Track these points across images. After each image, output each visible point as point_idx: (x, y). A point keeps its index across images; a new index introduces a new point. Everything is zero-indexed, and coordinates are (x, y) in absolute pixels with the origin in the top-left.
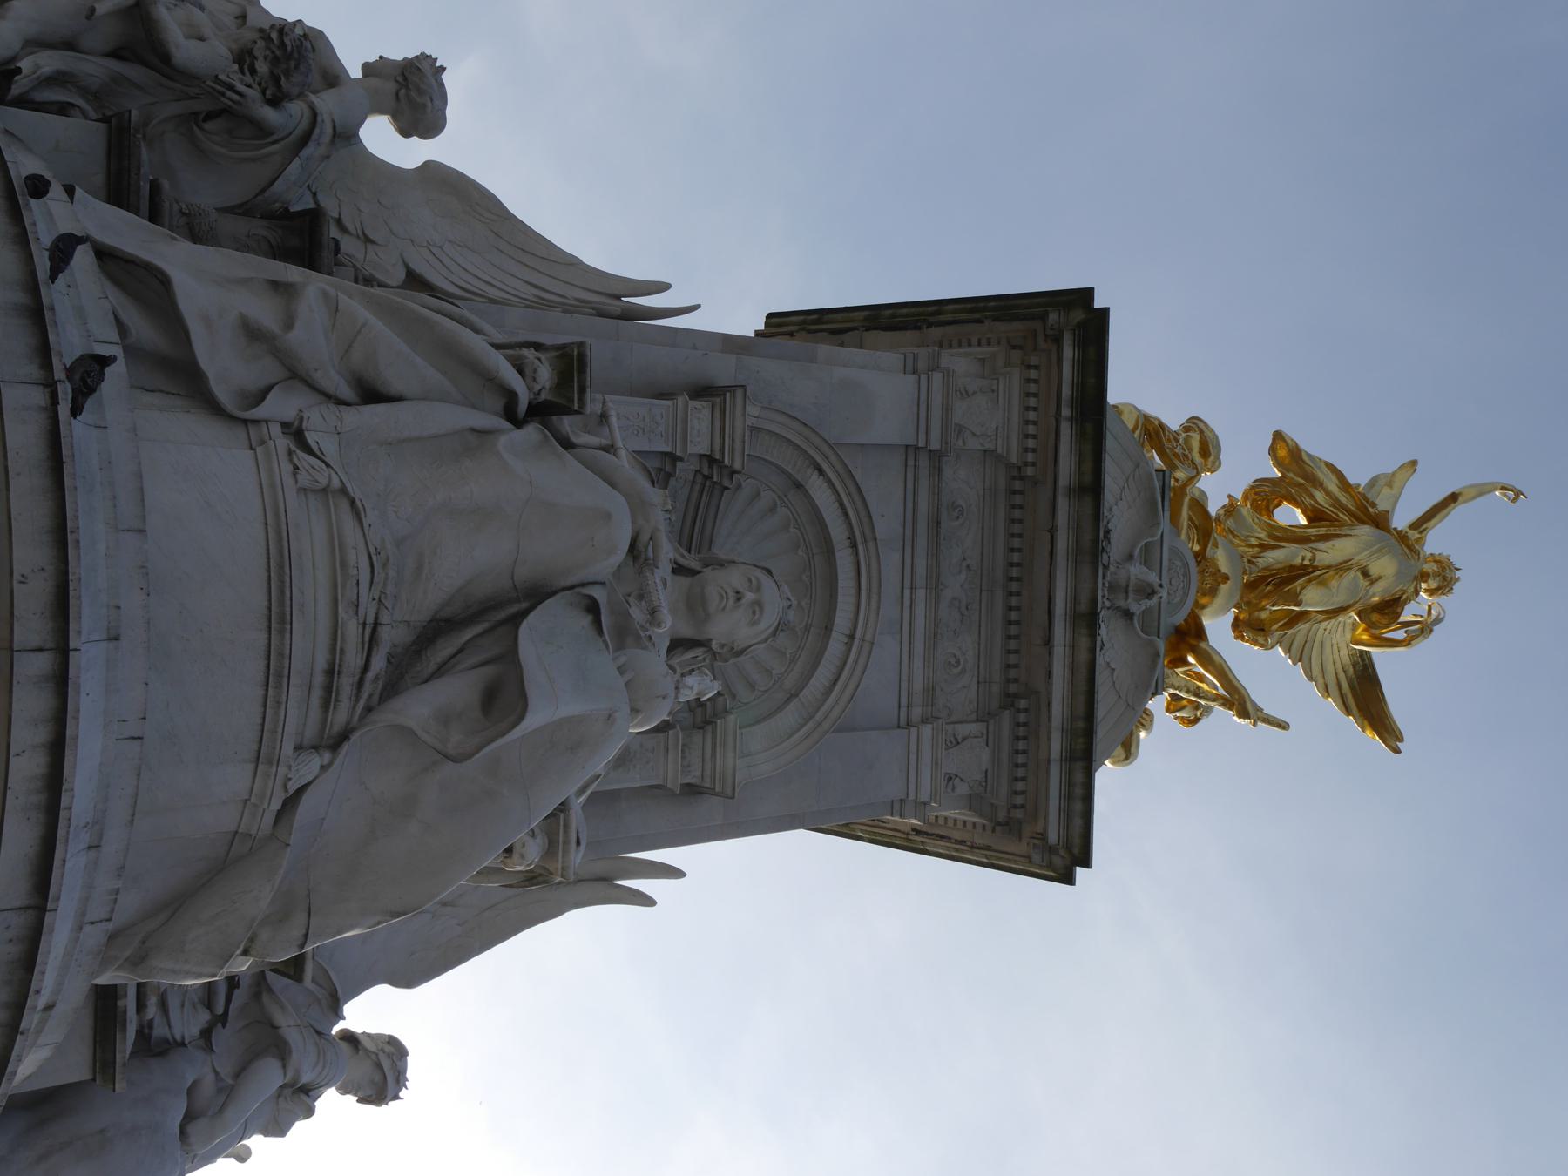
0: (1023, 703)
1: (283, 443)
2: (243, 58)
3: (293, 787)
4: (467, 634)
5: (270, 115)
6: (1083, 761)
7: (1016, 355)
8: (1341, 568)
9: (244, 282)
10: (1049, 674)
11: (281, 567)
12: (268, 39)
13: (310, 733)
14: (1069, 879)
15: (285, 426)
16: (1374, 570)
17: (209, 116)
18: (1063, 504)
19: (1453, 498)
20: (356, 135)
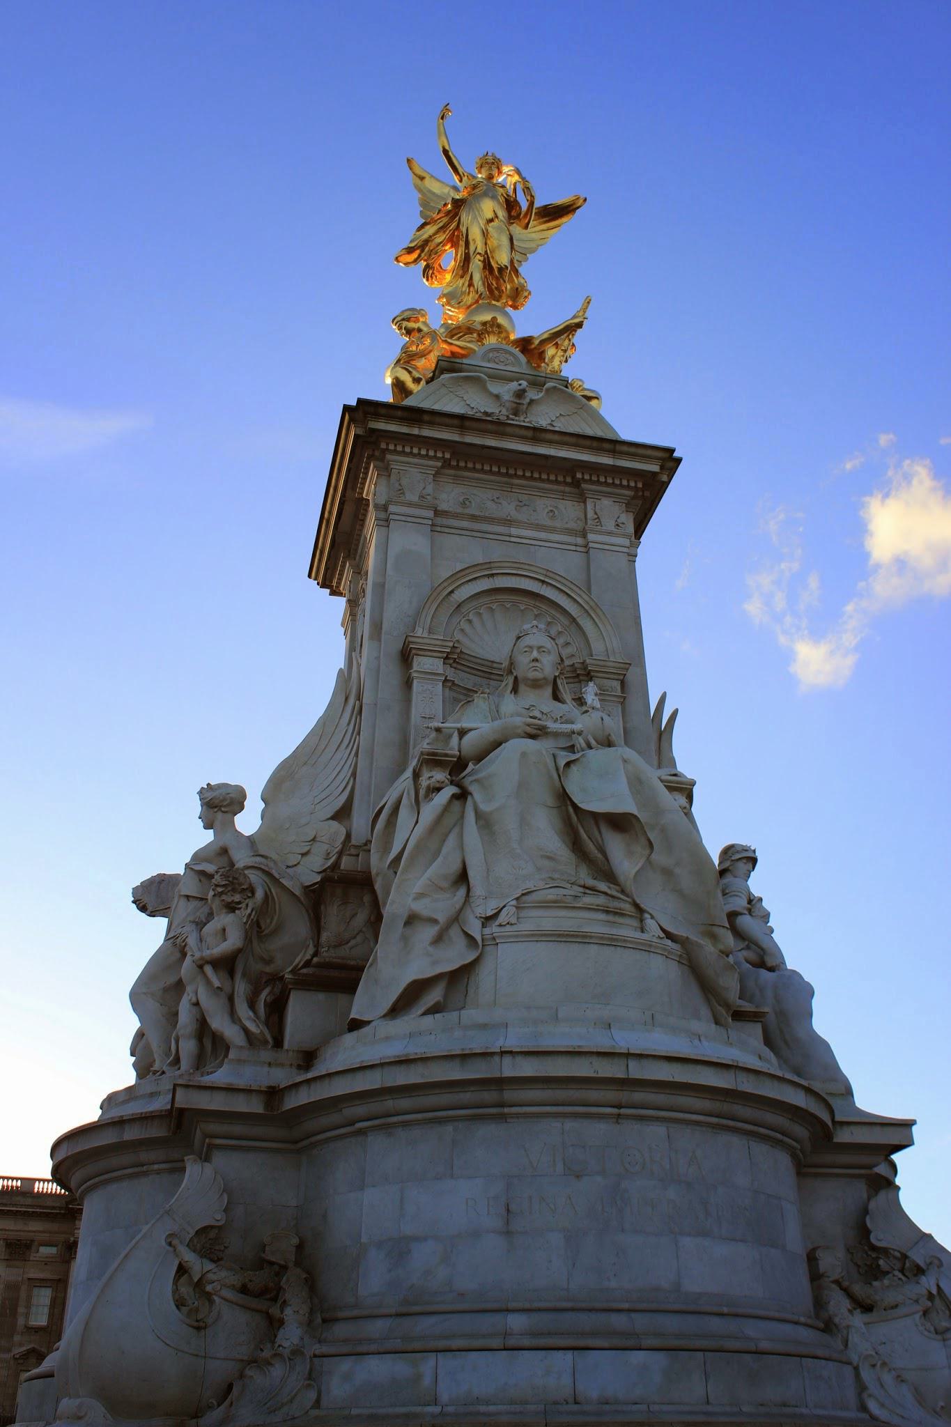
0: (579, 476)
1: (493, 929)
2: (231, 908)
3: (662, 935)
4: (584, 836)
5: (259, 894)
6: (614, 445)
8: (485, 234)
9: (405, 939)
10: (565, 459)
11: (559, 935)
12: (222, 893)
13: (635, 923)
14: (679, 461)
15: (484, 926)
16: (490, 215)
17: (259, 926)
18: (469, 439)
19: (446, 152)
20: (248, 837)
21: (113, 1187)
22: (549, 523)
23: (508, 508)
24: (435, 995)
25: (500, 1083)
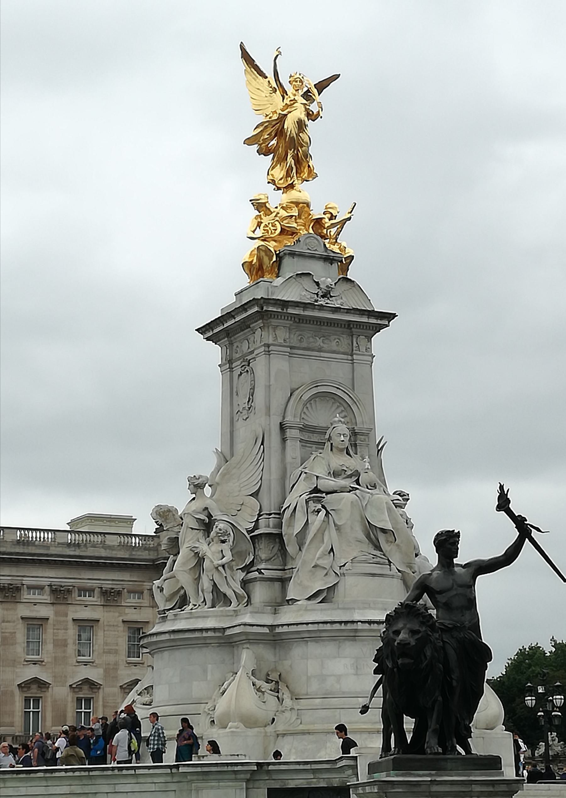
0: (352, 326)
2: (223, 542)
7: (265, 317)
15: (340, 569)
21: (191, 649)
22: (335, 348)
23: (319, 342)
24: (324, 594)
25: (356, 630)
